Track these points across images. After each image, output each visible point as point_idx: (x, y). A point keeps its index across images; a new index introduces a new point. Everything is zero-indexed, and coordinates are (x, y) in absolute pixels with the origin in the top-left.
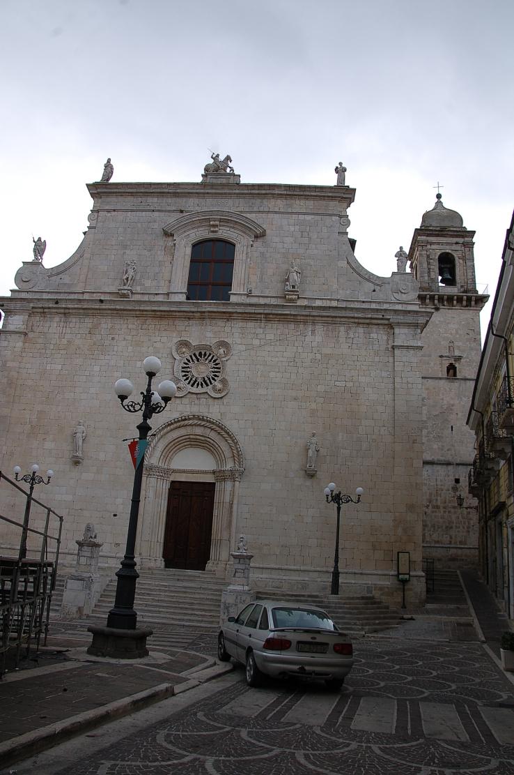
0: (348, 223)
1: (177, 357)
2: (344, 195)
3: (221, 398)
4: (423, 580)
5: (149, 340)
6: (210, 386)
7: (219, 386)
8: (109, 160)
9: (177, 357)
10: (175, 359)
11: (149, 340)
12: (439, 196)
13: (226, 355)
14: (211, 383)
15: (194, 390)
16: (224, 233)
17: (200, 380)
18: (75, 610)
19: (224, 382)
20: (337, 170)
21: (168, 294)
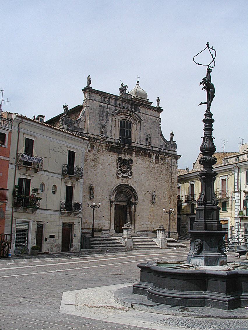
0: (161, 122)
1: (119, 163)
2: (160, 110)
3: (131, 178)
4: (177, 233)
5: (110, 156)
6: (127, 174)
7: (130, 174)
8: (89, 76)
9: (119, 163)
10: (118, 164)
11: (110, 156)
12: (138, 82)
13: (131, 163)
14: (127, 173)
15: (124, 175)
16: (130, 119)
17: (124, 171)
18: (130, 247)
19: (131, 173)
20: (157, 100)
21: (115, 139)
